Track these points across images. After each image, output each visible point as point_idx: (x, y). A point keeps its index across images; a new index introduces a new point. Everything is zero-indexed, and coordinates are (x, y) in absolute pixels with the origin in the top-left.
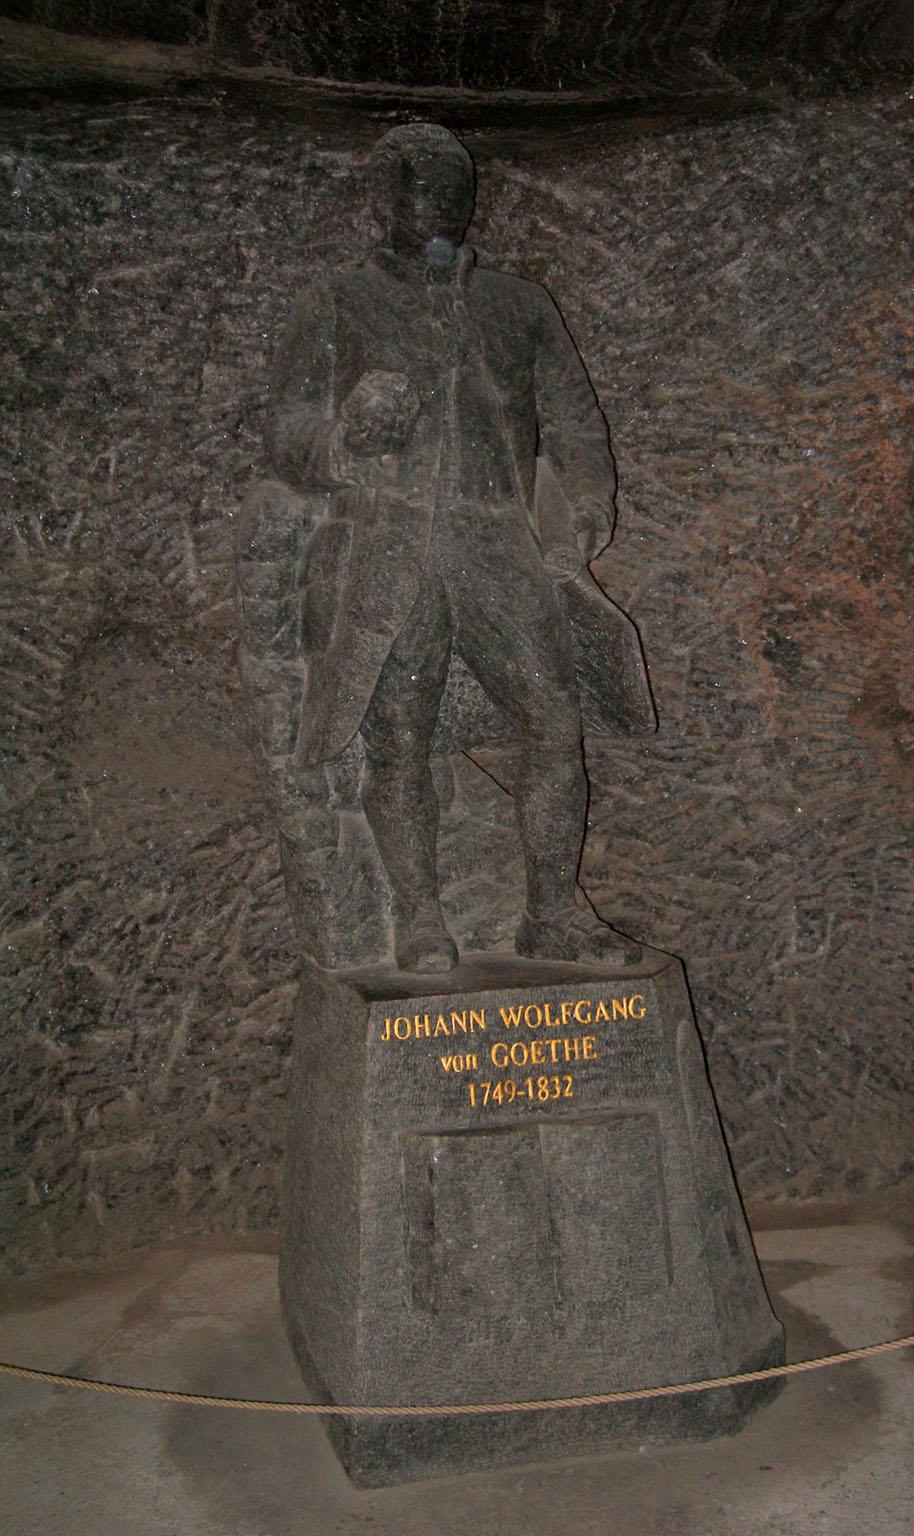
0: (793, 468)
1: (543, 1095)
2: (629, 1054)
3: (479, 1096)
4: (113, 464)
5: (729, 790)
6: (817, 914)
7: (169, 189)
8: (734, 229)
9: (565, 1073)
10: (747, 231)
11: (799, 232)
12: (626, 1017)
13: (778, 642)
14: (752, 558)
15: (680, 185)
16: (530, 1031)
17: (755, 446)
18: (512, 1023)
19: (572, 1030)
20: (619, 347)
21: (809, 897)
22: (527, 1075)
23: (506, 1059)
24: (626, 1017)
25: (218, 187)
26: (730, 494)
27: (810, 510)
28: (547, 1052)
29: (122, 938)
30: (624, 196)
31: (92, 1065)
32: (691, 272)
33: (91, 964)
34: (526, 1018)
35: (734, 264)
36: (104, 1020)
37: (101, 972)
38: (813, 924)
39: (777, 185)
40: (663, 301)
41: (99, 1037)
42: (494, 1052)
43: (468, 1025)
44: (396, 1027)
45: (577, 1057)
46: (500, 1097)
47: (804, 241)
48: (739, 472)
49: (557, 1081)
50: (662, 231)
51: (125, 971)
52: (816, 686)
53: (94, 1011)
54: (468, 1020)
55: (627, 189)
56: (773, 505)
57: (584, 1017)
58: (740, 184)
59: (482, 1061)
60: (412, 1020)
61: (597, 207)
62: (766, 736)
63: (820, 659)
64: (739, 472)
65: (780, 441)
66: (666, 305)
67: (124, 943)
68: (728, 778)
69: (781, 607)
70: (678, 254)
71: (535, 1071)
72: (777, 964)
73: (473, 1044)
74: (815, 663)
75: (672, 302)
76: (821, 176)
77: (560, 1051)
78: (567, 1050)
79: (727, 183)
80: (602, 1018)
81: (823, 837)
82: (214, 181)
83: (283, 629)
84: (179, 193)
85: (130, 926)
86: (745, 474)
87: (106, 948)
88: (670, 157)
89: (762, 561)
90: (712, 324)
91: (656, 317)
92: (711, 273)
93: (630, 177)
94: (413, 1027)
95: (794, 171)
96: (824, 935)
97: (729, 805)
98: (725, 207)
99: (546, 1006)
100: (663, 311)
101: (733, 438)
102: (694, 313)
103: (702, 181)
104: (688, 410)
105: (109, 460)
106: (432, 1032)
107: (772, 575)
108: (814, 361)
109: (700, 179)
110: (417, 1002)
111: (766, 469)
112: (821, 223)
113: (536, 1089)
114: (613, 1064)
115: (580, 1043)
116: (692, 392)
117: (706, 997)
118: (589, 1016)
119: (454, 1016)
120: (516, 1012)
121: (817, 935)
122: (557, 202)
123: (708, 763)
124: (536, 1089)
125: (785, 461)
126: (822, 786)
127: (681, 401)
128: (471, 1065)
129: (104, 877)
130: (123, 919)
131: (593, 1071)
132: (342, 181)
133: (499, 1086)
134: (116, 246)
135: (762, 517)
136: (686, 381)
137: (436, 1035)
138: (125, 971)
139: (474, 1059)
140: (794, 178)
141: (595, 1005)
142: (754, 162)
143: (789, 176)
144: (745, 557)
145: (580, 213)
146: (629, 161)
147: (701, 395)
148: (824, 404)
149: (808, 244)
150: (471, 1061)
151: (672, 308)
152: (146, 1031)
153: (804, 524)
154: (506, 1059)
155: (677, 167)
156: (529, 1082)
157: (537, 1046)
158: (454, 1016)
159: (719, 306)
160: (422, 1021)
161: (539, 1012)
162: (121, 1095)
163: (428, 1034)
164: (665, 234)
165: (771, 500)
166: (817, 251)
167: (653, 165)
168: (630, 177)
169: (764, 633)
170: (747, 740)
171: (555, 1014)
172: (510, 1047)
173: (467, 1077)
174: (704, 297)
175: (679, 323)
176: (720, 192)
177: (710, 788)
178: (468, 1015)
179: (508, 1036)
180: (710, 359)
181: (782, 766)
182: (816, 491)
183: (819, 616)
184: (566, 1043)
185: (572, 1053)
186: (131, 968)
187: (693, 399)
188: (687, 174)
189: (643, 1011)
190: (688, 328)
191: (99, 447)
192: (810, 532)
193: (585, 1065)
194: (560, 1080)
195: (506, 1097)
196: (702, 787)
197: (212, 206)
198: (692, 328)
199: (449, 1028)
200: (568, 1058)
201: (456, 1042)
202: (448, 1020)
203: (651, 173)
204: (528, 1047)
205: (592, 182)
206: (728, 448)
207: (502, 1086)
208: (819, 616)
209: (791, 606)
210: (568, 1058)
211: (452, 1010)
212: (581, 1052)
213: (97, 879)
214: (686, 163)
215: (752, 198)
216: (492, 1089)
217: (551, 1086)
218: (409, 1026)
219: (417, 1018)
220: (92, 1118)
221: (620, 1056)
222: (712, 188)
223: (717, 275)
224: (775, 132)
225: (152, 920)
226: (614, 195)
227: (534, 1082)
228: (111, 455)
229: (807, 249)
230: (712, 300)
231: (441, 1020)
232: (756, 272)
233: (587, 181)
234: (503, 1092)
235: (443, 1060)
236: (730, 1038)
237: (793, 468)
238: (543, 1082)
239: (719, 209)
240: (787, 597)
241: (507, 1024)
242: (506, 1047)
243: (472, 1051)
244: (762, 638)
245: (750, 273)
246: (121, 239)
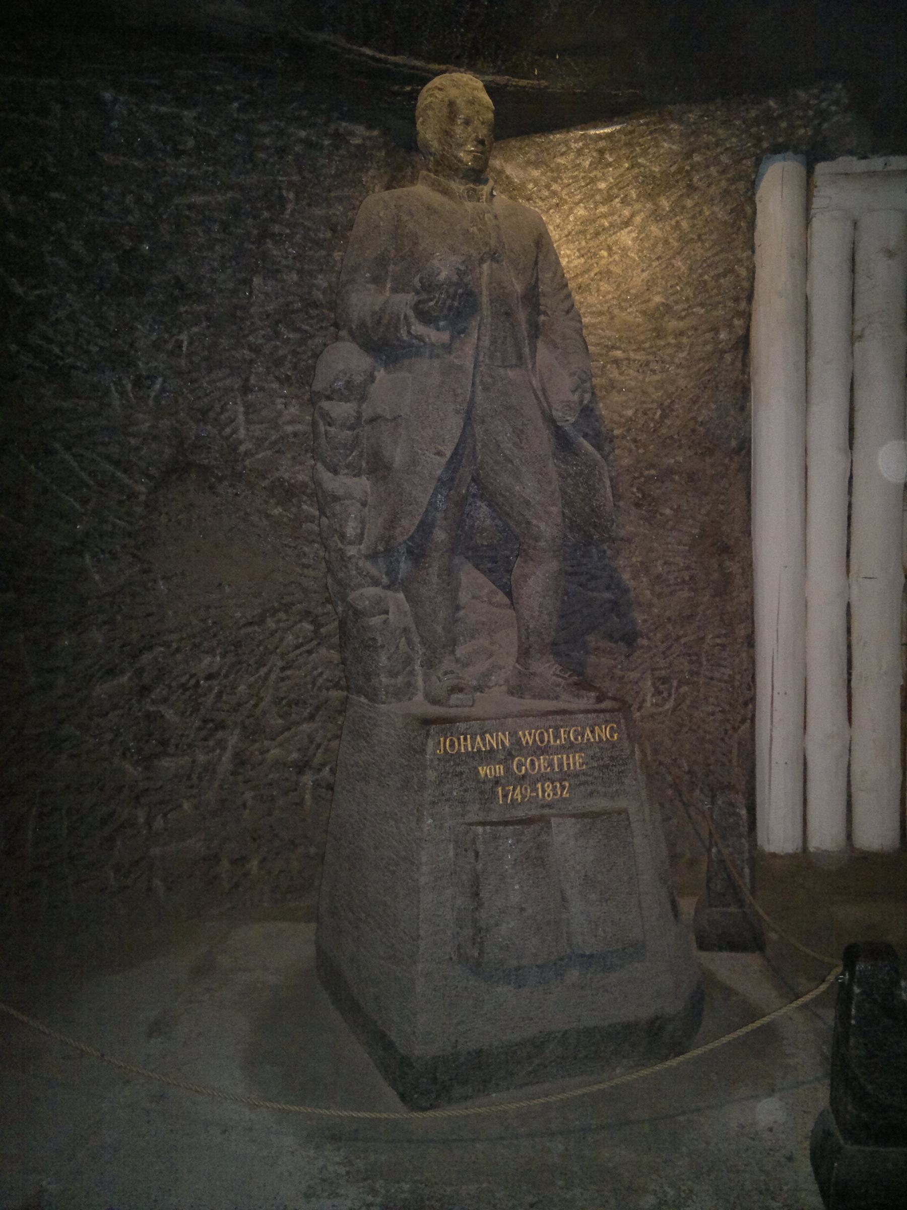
0: (657, 377)
1: (549, 795)
2: (607, 766)
3: (505, 796)
4: (185, 344)
5: (607, 595)
6: (665, 680)
8: (629, 204)
9: (565, 780)
10: (638, 206)
11: (672, 210)
12: (605, 739)
13: (643, 496)
14: (628, 438)
15: (596, 168)
16: (539, 748)
17: (634, 361)
18: (527, 743)
19: (570, 747)
21: (661, 669)
22: (538, 781)
23: (524, 768)
24: (605, 739)
25: (267, 141)
26: (616, 394)
27: (669, 407)
28: (551, 764)
29: (187, 689)
30: (555, 175)
31: (160, 783)
32: (597, 234)
33: (163, 709)
34: (537, 738)
35: (626, 230)
36: (171, 750)
37: (170, 714)
38: (662, 687)
39: (661, 173)
40: (577, 254)
41: (166, 762)
42: (515, 763)
43: (497, 744)
44: (448, 743)
45: (572, 768)
46: (519, 797)
47: (676, 215)
48: (623, 378)
49: (558, 785)
50: (579, 203)
51: (188, 713)
52: (668, 527)
53: (164, 743)
54: (497, 739)
55: (558, 169)
56: (644, 402)
57: (576, 739)
58: (636, 170)
59: (508, 769)
60: (459, 739)
61: (536, 182)
62: (634, 559)
63: (671, 508)
64: (623, 378)
65: (651, 358)
66: (579, 257)
67: (188, 693)
68: (608, 588)
69: (646, 473)
71: (543, 778)
72: (638, 714)
73: (501, 756)
74: (668, 511)
75: (583, 256)
76: (693, 167)
77: (561, 765)
78: (565, 763)
79: (628, 169)
80: (588, 740)
81: (671, 628)
82: (265, 135)
83: (354, 454)
84: (237, 141)
85: (193, 682)
86: (626, 380)
87: (174, 697)
88: (591, 146)
89: (635, 441)
90: (609, 272)
91: (572, 265)
92: (611, 236)
94: (459, 744)
95: (675, 163)
96: (670, 695)
97: (608, 605)
98: (624, 187)
99: (551, 730)
100: (576, 262)
101: (618, 354)
102: (597, 264)
103: (611, 166)
105: (182, 341)
106: (473, 748)
107: (641, 451)
108: (676, 303)
109: (609, 165)
110: (462, 726)
111: (640, 377)
112: (689, 203)
113: (544, 791)
114: (596, 774)
115: (574, 757)
116: (593, 321)
118: (579, 738)
119: (487, 736)
120: (530, 734)
121: (665, 694)
122: (507, 177)
123: (594, 577)
124: (544, 791)
125: (654, 372)
126: (671, 593)
128: (500, 772)
129: (175, 645)
130: (187, 676)
131: (583, 778)
132: (358, 147)
133: (519, 788)
134: (190, 177)
135: (637, 410)
137: (475, 750)
138: (188, 713)
139: (502, 768)
140: (673, 169)
141: (584, 728)
142: (648, 154)
143: (671, 166)
144: (624, 437)
145: (523, 185)
147: (600, 323)
148: (682, 333)
149: (678, 218)
150: (500, 770)
151: (582, 260)
152: (202, 758)
153: (664, 416)
154: (524, 768)
155: (595, 154)
156: (539, 785)
157: (544, 759)
158: (487, 736)
159: (614, 260)
160: (465, 739)
161: (546, 734)
162: (180, 806)
163: (470, 749)
164: (582, 205)
165: (643, 399)
166: (685, 224)
167: (579, 152)
168: (561, 161)
169: (635, 490)
170: (621, 562)
171: (557, 736)
172: (526, 760)
173: (497, 782)
174: (604, 253)
175: (588, 271)
176: (622, 175)
177: (595, 594)
178: (497, 735)
179: (525, 751)
180: (607, 298)
181: (644, 580)
182: (673, 393)
183: (672, 480)
184: (565, 756)
185: (568, 764)
186: (192, 712)
189: (616, 736)
190: (592, 274)
191: (175, 331)
192: (668, 422)
193: (576, 775)
194: (561, 785)
195: (524, 797)
196: (590, 593)
197: (262, 155)
199: (485, 745)
200: (566, 769)
201: (489, 756)
202: (483, 739)
203: (576, 158)
204: (539, 759)
205: (536, 164)
206: (616, 362)
207: (521, 789)
208: (672, 480)
209: (653, 472)
210: (566, 769)
211: (486, 732)
212: (575, 764)
213: (169, 647)
214: (601, 152)
215: (643, 181)
216: (514, 790)
217: (554, 788)
218: (456, 744)
219: (462, 737)
220: (159, 822)
221: (600, 768)
223: (614, 238)
224: (665, 131)
225: (209, 677)
226: (549, 174)
228: (184, 337)
229: (677, 222)
230: (610, 255)
231: (479, 739)
232: (640, 237)
233: (529, 163)
234: (521, 793)
235: (480, 769)
237: (657, 377)
238: (548, 786)
239: (620, 189)
240: (652, 466)
241: (524, 743)
242: (523, 760)
243: (499, 763)
244: (633, 493)
245: (637, 237)
246: (193, 171)
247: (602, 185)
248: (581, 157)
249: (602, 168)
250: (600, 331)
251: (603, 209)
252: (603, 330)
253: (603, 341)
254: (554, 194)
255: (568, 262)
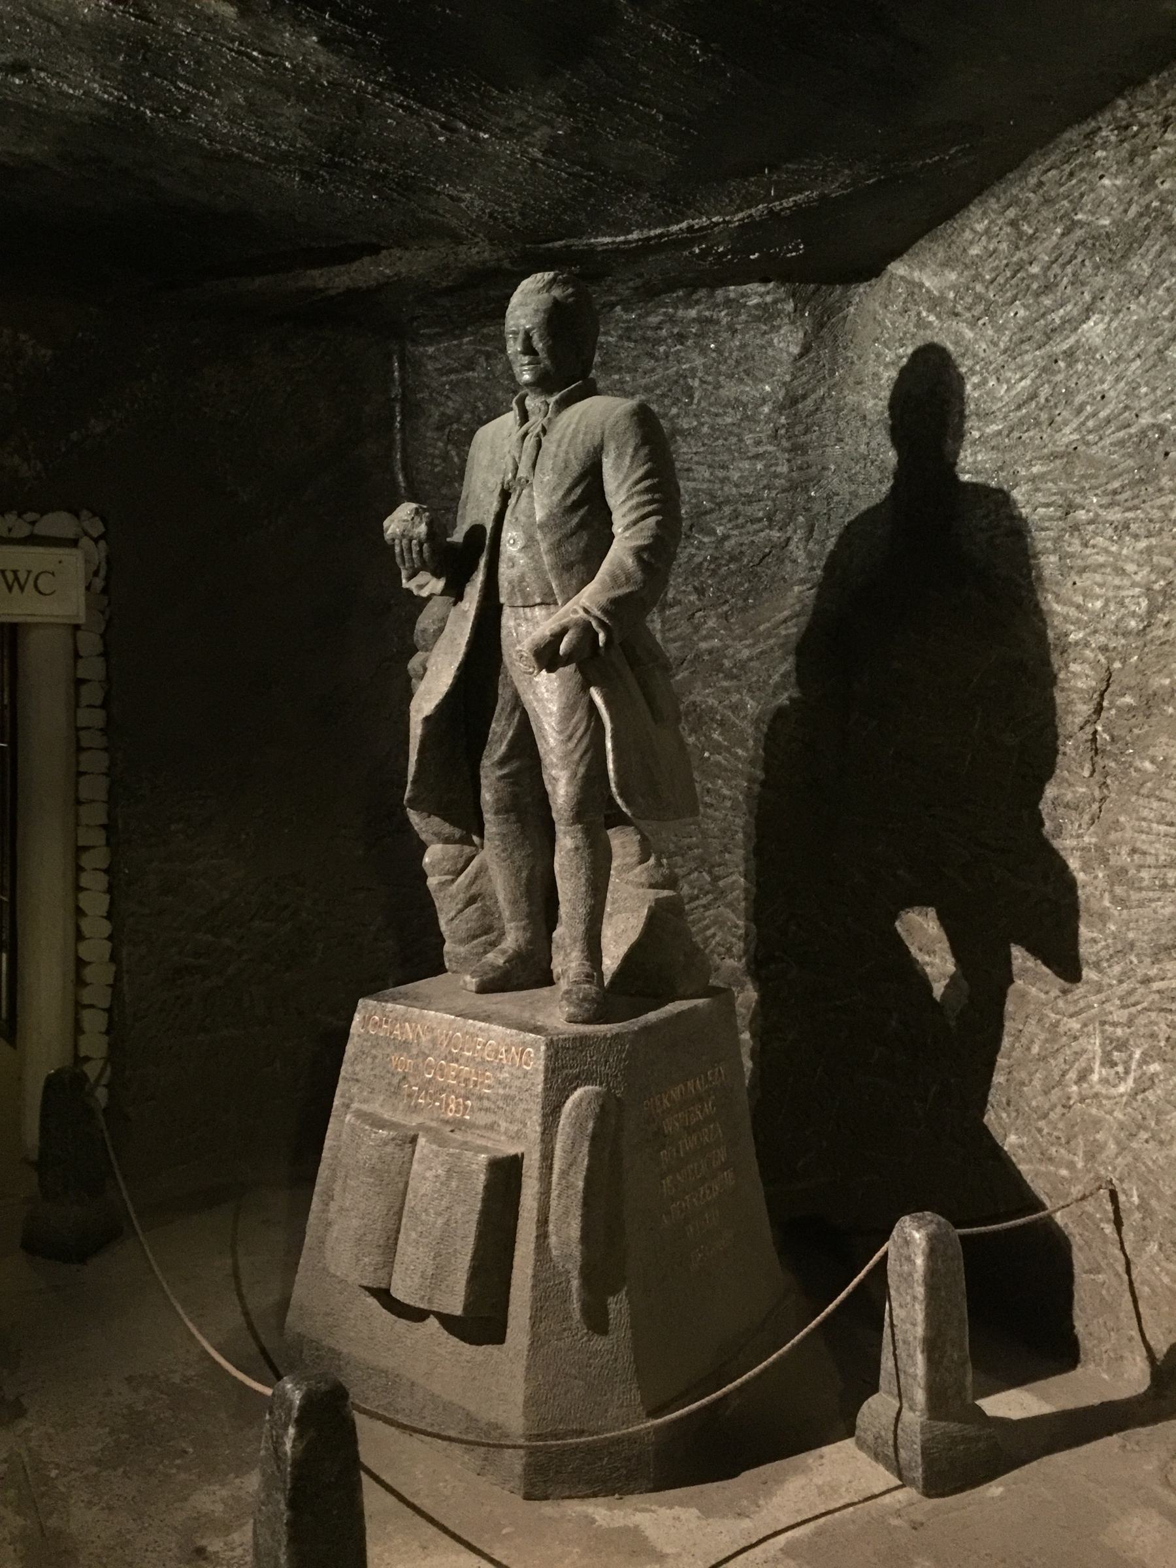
7: (629, 339)
9: (468, 1099)
20: (979, 429)
25: (664, 332)
70: (1030, 322)
82: (659, 327)
93: (974, 251)
104: (1037, 490)
109: (1031, 239)
117: (1004, 1100)
127: (1033, 479)
131: (486, 1103)
136: (1040, 459)
146: (968, 235)
187: (1042, 477)
188: (1020, 234)
198: (1047, 400)
205: (947, 264)
222: (1049, 244)
227: (447, 1097)
230: (1070, 365)
236: (1021, 1152)
247: (1035, 269)
248: (995, 240)
249: (1027, 246)
250: (1050, 484)
251: (1047, 301)
252: (1054, 481)
253: (1054, 498)
254: (979, 298)
255: (1008, 390)
